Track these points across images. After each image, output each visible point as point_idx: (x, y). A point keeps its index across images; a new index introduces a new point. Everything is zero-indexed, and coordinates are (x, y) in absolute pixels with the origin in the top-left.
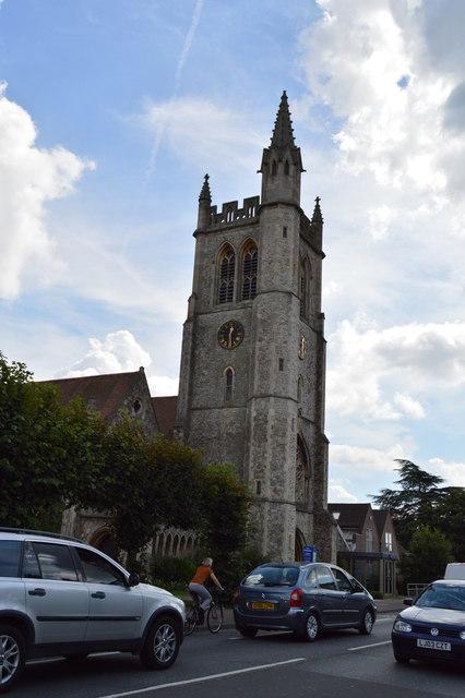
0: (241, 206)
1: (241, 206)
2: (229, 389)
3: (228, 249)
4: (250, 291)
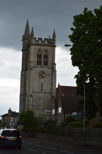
0: (43, 40)
1: (43, 40)
3: (40, 50)
4: (46, 63)
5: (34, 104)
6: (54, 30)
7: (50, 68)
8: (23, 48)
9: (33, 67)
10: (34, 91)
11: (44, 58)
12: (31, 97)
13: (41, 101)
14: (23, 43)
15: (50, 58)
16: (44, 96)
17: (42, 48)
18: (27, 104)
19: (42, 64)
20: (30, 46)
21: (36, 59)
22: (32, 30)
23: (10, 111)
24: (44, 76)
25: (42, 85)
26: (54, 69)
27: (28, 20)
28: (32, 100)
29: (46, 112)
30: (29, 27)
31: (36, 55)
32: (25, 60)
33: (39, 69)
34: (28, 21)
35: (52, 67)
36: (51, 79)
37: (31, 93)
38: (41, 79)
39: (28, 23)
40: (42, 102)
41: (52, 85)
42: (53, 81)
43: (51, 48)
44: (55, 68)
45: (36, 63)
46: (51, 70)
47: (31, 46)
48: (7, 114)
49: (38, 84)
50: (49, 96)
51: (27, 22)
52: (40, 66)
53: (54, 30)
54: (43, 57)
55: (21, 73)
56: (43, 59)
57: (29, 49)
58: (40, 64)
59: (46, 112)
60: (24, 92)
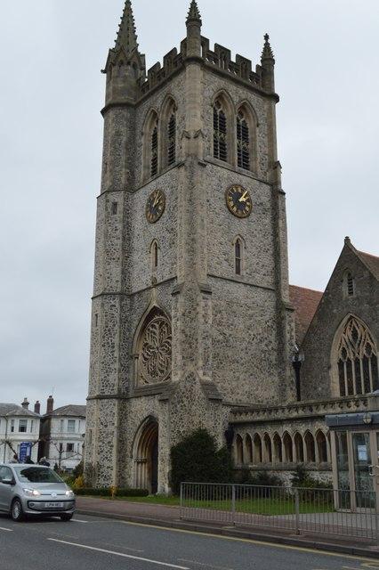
2: (238, 261)
3: (220, 98)
4: (244, 161)
6: (267, 37)
12: (206, 296)
13: (240, 324)
14: (108, 83)
15: (259, 137)
16: (249, 302)
20: (183, 69)
24: (247, 208)
25: (238, 246)
32: (127, 144)
36: (269, 228)
38: (237, 220)
40: (242, 326)
43: (261, 100)
49: (222, 239)
50: (266, 304)
51: (123, 6)
53: (267, 37)
56: (234, 143)
58: (223, 157)
60: (123, 280)
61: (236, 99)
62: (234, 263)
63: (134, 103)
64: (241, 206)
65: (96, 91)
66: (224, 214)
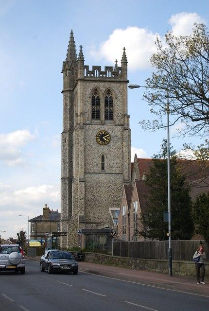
0: (103, 70)
1: (103, 70)
3: (95, 91)
4: (109, 116)
5: (89, 196)
6: (124, 49)
7: (119, 125)
8: (64, 88)
9: (84, 124)
10: (87, 171)
11: (106, 105)
12: (82, 183)
14: (64, 77)
17: (102, 87)
18: (74, 197)
19: (103, 116)
21: (89, 108)
22: (81, 51)
23: (46, 210)
24: (107, 140)
26: (126, 126)
27: (72, 31)
28: (84, 189)
29: (111, 211)
30: (75, 44)
31: (90, 100)
33: (95, 128)
34: (72, 33)
35: (121, 122)
37: (82, 176)
39: (72, 38)
41: (123, 158)
42: (124, 148)
43: (118, 84)
44: (128, 125)
45: (90, 116)
46: (120, 128)
47: (79, 83)
48: (40, 217)
52: (98, 121)
53: (124, 49)
54: (102, 104)
55: (63, 137)
57: (75, 89)
58: (98, 117)
59: (111, 211)
61: (104, 89)
62: (100, 165)
63: (72, 89)
64: (103, 140)
65: (58, 81)
66: (95, 145)
